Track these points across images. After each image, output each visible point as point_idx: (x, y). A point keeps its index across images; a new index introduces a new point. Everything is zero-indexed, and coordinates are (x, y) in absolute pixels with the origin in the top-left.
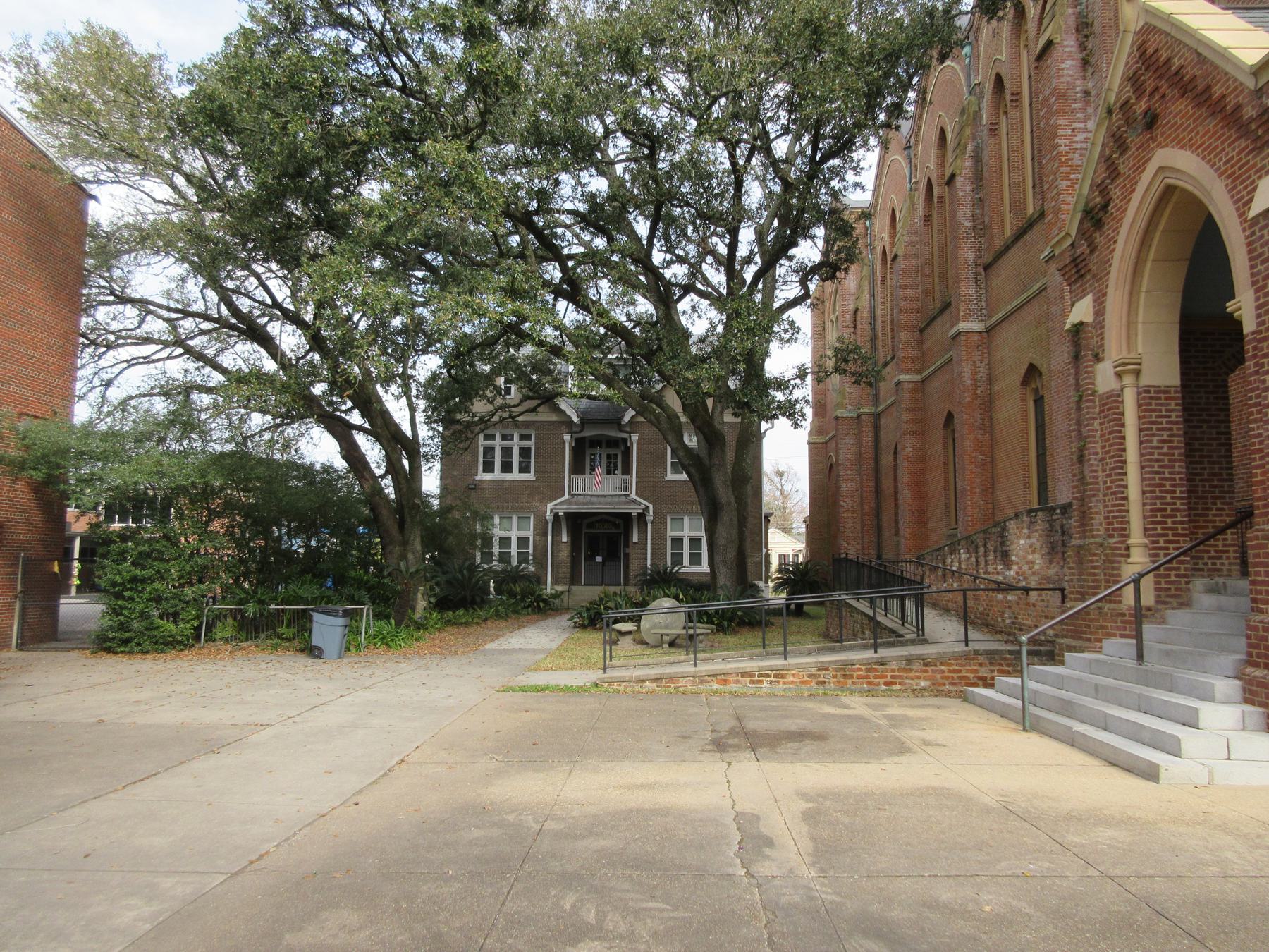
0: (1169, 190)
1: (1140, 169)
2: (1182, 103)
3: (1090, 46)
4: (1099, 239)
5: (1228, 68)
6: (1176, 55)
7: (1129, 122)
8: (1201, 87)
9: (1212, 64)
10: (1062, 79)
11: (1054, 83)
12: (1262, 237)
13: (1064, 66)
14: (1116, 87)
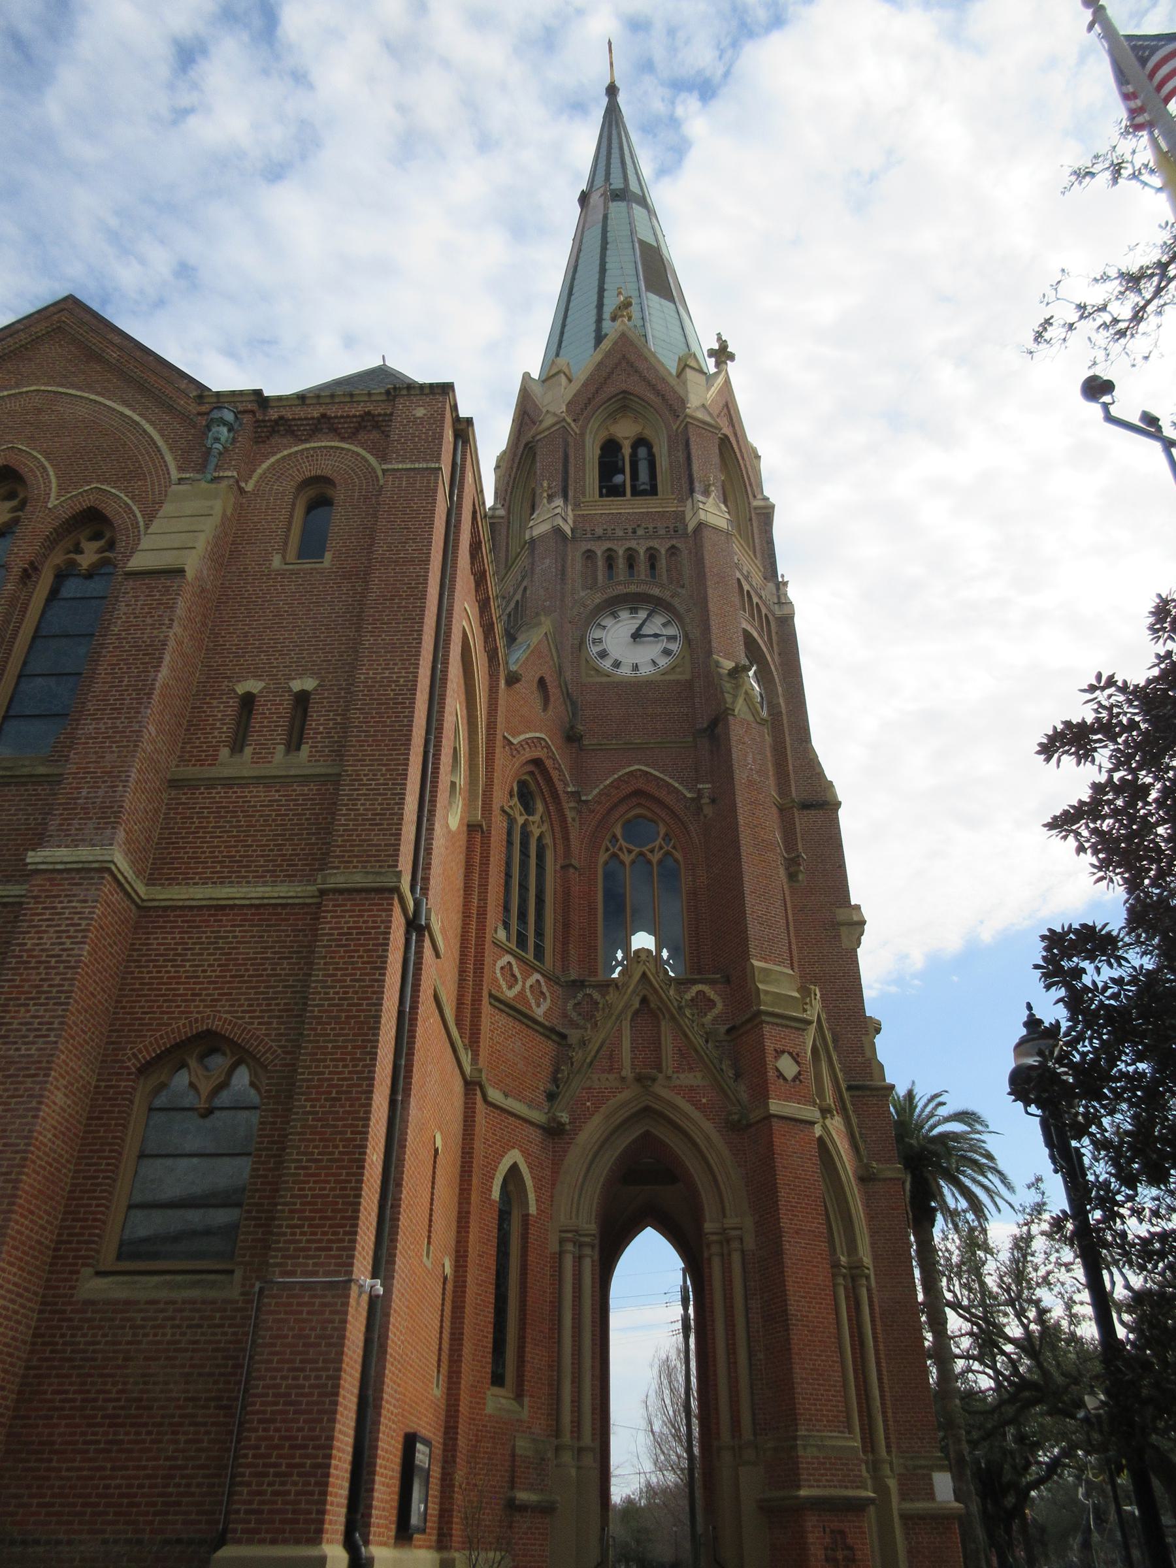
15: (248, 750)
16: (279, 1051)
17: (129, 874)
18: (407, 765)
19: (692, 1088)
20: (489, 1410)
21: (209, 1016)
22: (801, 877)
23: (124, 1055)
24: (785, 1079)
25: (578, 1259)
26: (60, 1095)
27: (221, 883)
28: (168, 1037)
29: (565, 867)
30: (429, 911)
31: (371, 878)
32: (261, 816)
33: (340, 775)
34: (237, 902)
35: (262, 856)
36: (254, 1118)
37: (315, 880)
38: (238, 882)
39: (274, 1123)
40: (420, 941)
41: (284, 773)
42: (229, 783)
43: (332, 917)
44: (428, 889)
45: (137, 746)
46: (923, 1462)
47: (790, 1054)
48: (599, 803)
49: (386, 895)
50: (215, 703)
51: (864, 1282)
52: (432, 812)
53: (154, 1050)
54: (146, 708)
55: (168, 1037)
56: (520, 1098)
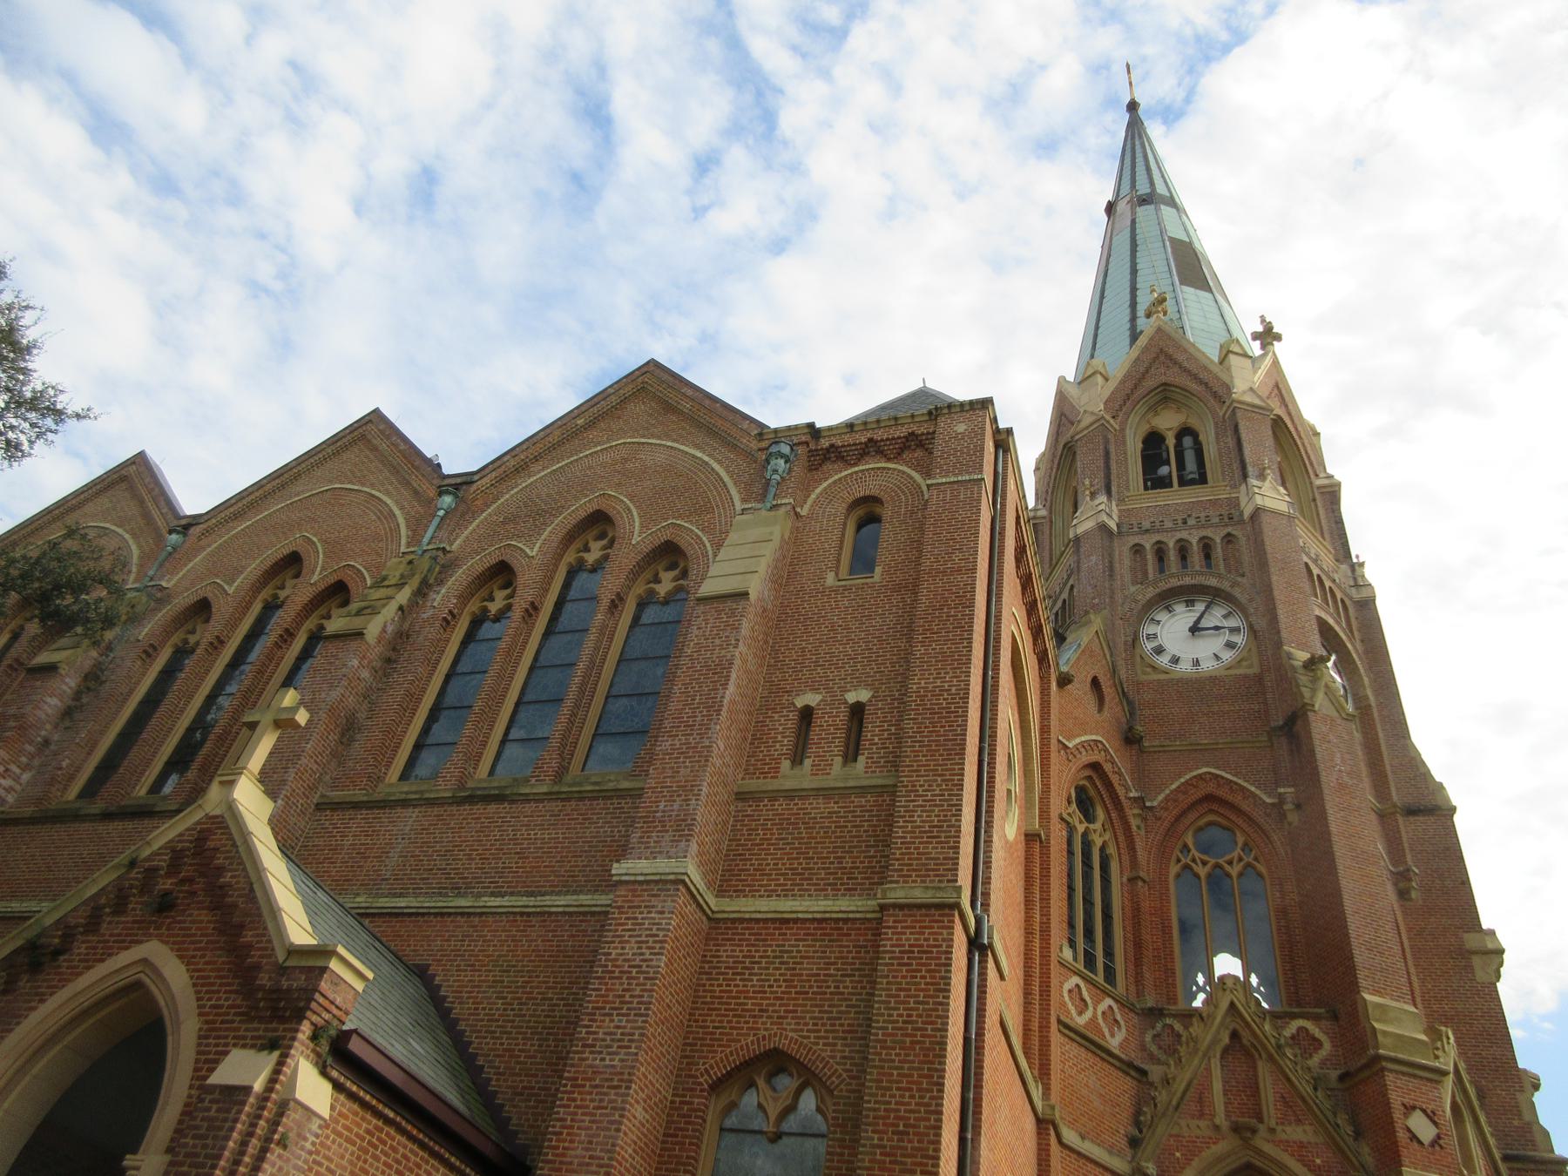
0: (138, 985)
1: (125, 943)
2: (206, 915)
3: (85, 700)
4: (24, 983)
5: (270, 926)
6: (231, 870)
7: (145, 888)
8: (236, 920)
9: (259, 908)
10: (38, 713)
11: (28, 709)
12: (208, 1110)
13: (49, 700)
14: (155, 846)
15: (808, 762)
16: (845, 1075)
17: (701, 885)
18: (963, 775)
19: (1301, 1145)
21: (775, 1034)
22: (1414, 895)
23: (697, 1070)
24: (1420, 1142)
26: (640, 1109)
27: (785, 896)
28: (738, 1055)
30: (991, 928)
31: (930, 893)
32: (822, 828)
33: (895, 786)
34: (800, 916)
35: (823, 869)
36: (821, 1146)
37: (875, 895)
38: (800, 896)
39: (842, 1155)
40: (983, 962)
41: (842, 785)
42: (790, 795)
43: (893, 933)
44: (989, 905)
45: (707, 761)
47: (1424, 1111)
48: (1166, 809)
49: (947, 911)
50: (776, 716)
52: (989, 824)
53: (725, 1067)
54: (716, 724)
55: (738, 1055)
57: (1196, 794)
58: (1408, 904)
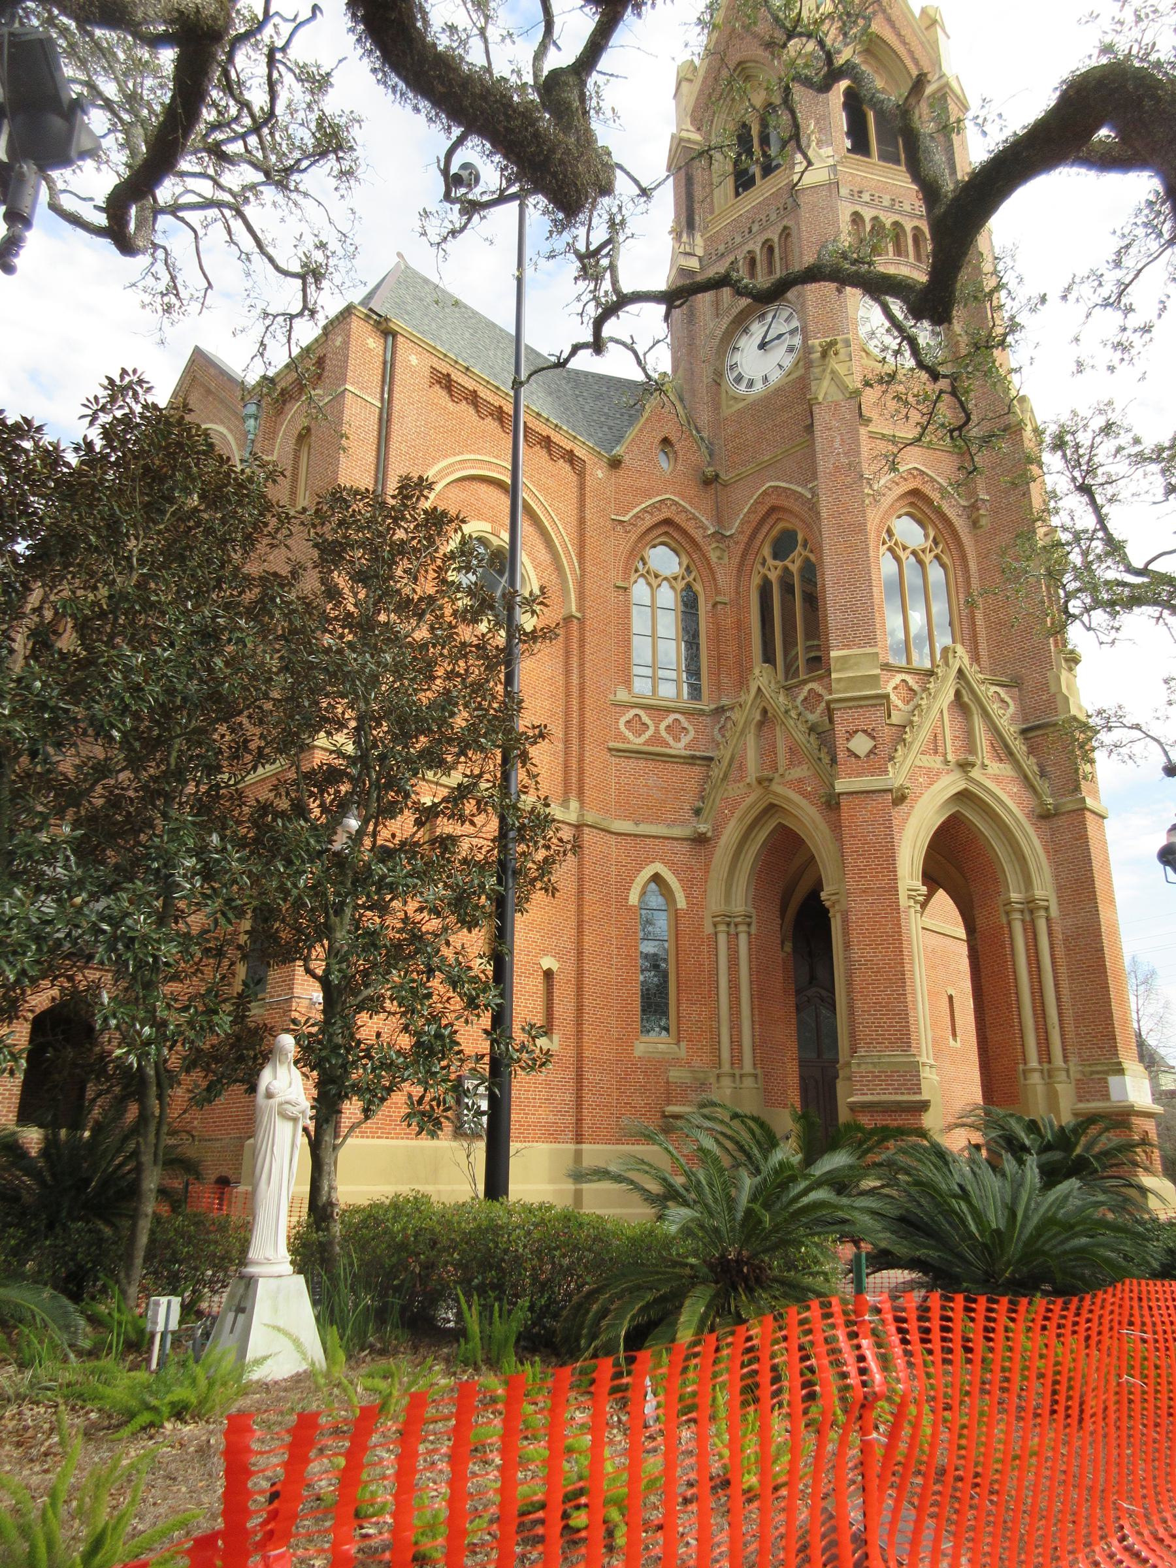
19: (800, 780)
20: (637, 1053)
22: (983, 521)
24: (857, 757)
25: (733, 938)
29: (715, 605)
46: (1099, 1068)
47: (865, 731)
48: (742, 532)
51: (1042, 913)
56: (656, 819)
57: (763, 510)
58: (979, 531)
